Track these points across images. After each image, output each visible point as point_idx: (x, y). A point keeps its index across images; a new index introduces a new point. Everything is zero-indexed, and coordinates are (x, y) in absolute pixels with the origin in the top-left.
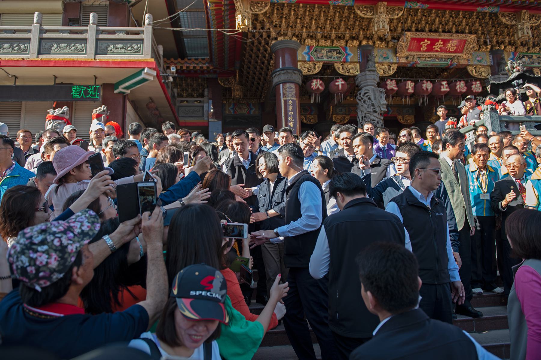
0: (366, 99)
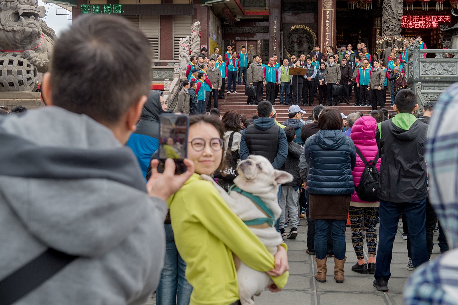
0: (388, 8)
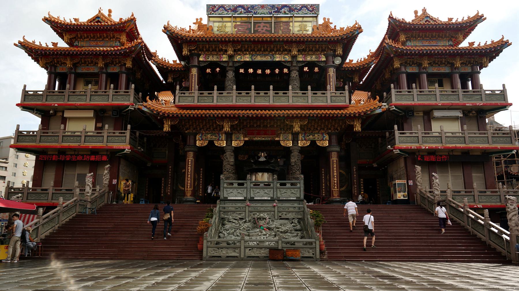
0: (225, 158)
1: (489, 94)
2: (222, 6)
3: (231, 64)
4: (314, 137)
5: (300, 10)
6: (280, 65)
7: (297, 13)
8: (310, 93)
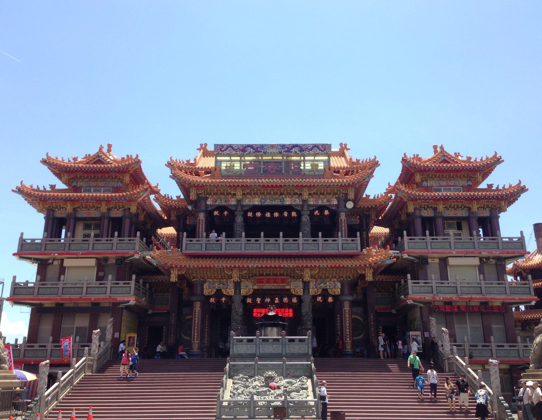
1: (506, 242)
2: (231, 146)
3: (239, 209)
4: (325, 285)
5: (311, 150)
6: (290, 208)
7: (308, 153)
8: (320, 239)
